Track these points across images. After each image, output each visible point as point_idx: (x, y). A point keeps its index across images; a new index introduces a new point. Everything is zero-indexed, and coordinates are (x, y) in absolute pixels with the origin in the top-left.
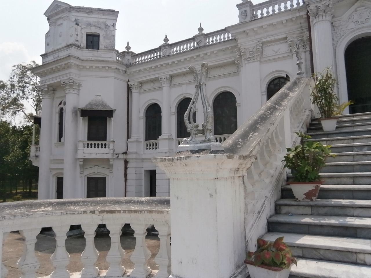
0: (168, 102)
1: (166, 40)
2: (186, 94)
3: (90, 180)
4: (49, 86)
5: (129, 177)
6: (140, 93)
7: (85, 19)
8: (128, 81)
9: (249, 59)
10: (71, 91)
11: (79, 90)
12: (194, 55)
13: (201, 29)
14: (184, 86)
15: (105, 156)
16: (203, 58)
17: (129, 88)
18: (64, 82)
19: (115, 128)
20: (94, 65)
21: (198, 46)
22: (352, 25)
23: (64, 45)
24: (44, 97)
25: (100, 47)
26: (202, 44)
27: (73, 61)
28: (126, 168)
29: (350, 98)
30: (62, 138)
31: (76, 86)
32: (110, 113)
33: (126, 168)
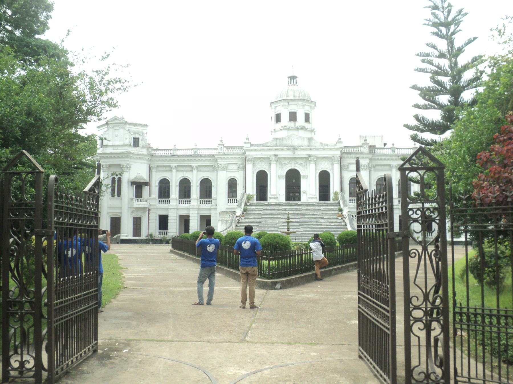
3: (134, 218)
5: (150, 218)
6: (156, 172)
7: (133, 129)
9: (222, 169)
12: (193, 159)
14: (185, 172)
15: (146, 206)
17: (150, 168)
19: (145, 190)
20: (138, 156)
22: (259, 166)
23: (121, 143)
25: (140, 145)
26: (196, 154)
27: (131, 155)
28: (149, 213)
29: (257, 193)
31: (128, 167)
32: (147, 184)
33: (149, 213)
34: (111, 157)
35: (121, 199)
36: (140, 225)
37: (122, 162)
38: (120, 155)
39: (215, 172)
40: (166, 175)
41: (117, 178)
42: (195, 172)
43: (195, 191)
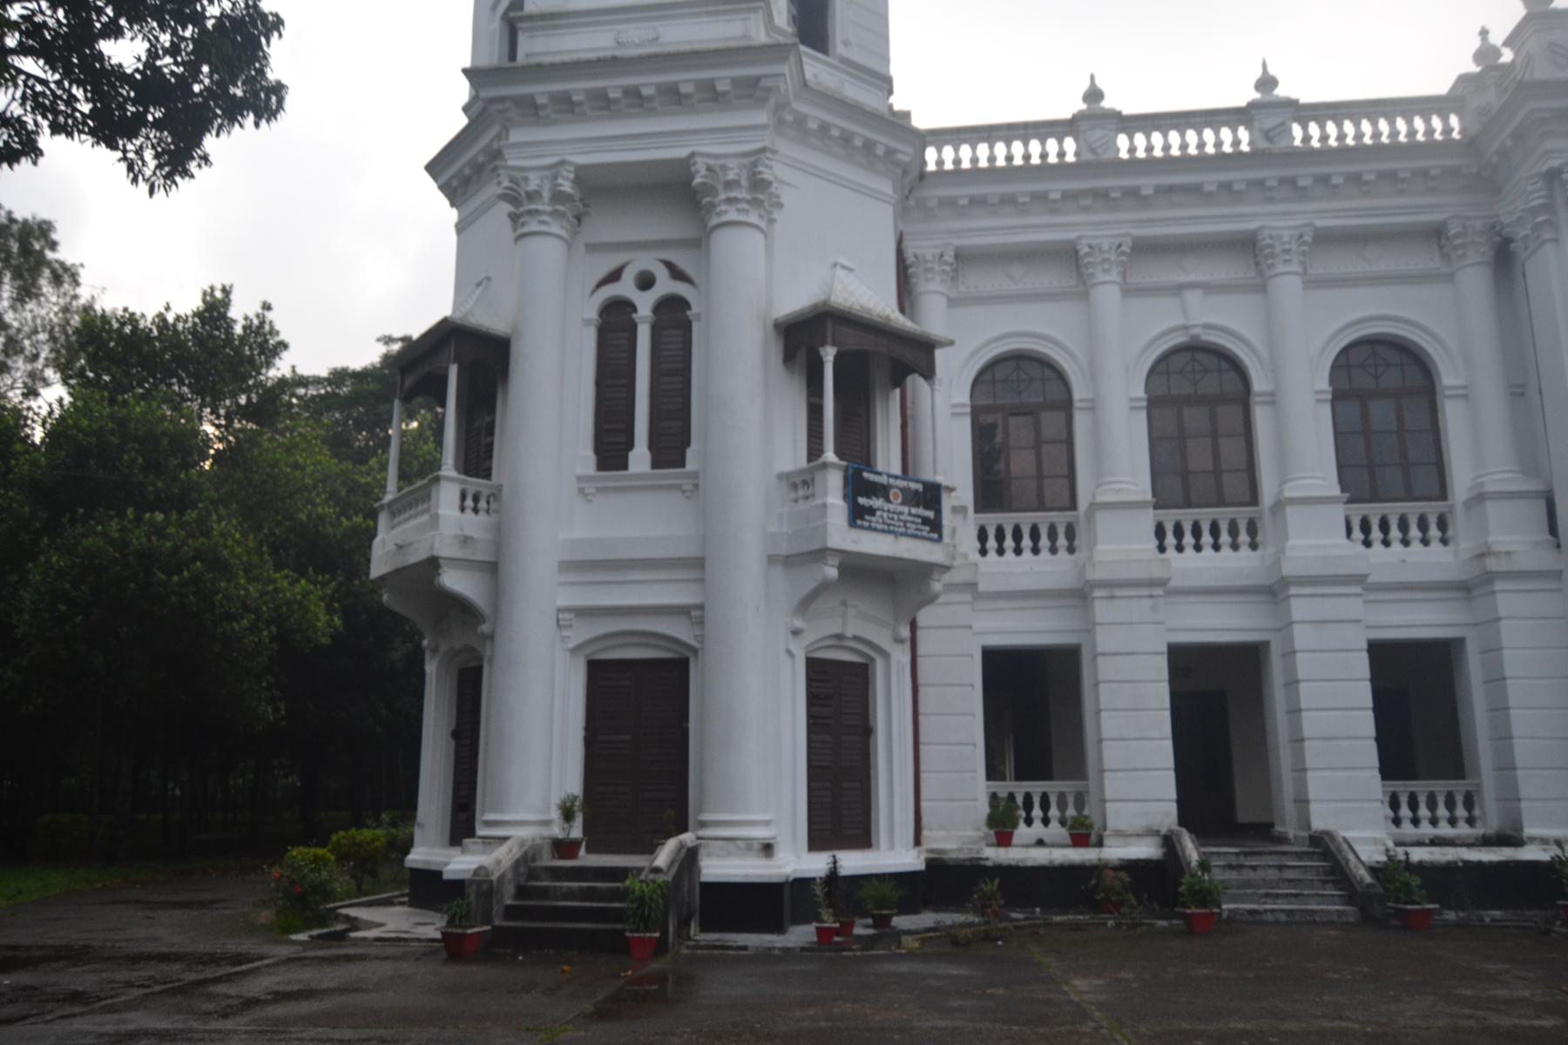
0: (1111, 353)
1: (1093, 95)
2: (1207, 326)
4: (583, 176)
6: (952, 302)
8: (899, 243)
10: (753, 218)
11: (771, 221)
13: (1266, 83)
14: (1194, 298)
16: (1302, 194)
18: (709, 169)
21: (1262, 144)
24: (543, 228)
25: (840, 49)
26: (1281, 144)
30: (632, 455)
34: (603, 104)
35: (695, 488)
36: (867, 731)
37: (702, 139)
38: (686, 79)
39: (1475, 280)
40: (1041, 325)
41: (645, 304)
42: (1287, 285)
43: (1299, 442)
